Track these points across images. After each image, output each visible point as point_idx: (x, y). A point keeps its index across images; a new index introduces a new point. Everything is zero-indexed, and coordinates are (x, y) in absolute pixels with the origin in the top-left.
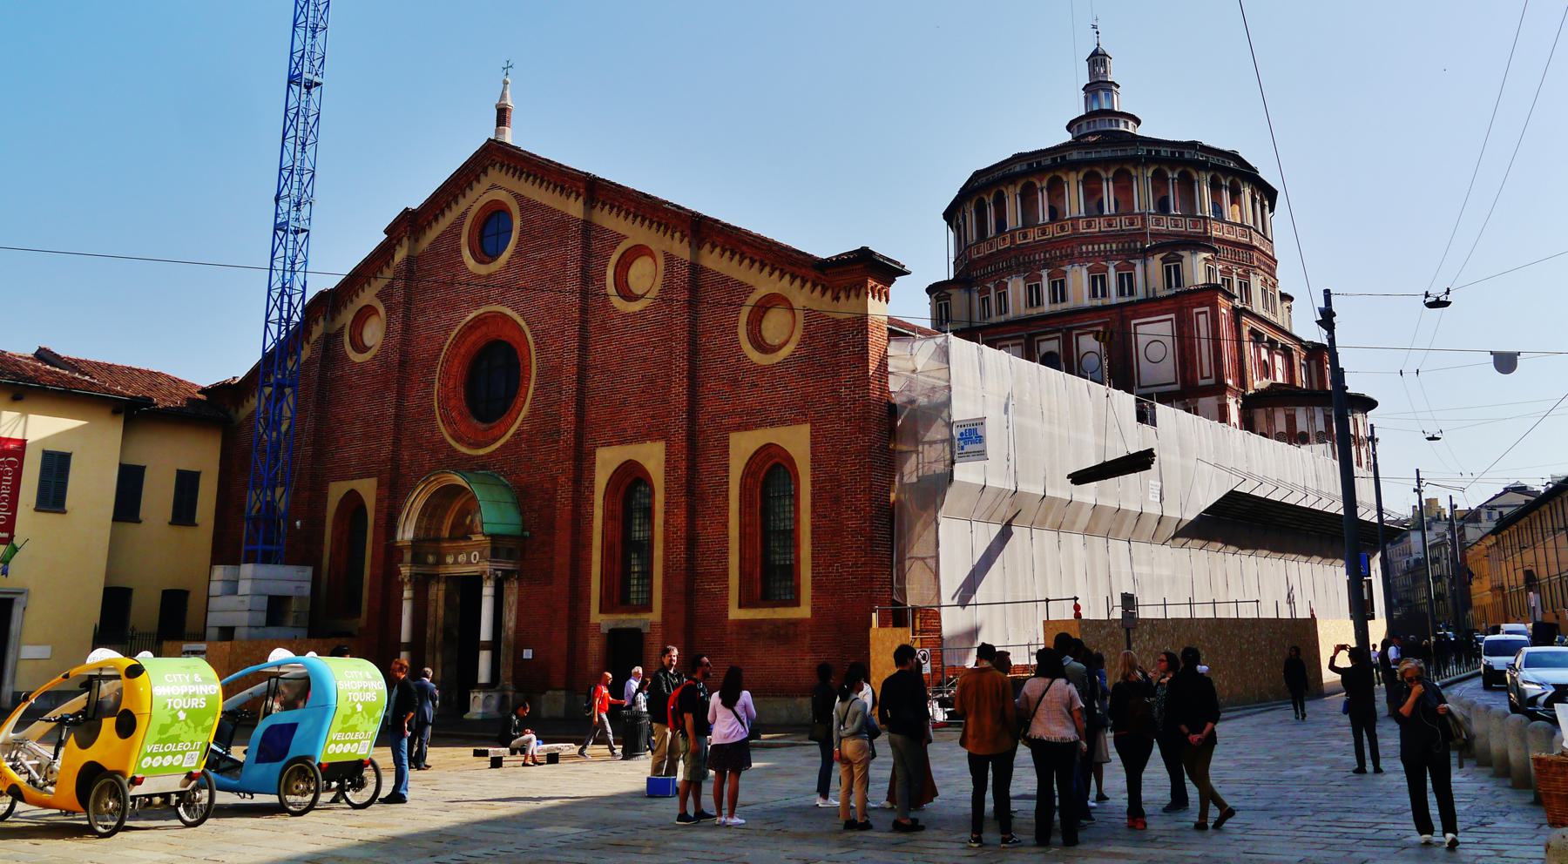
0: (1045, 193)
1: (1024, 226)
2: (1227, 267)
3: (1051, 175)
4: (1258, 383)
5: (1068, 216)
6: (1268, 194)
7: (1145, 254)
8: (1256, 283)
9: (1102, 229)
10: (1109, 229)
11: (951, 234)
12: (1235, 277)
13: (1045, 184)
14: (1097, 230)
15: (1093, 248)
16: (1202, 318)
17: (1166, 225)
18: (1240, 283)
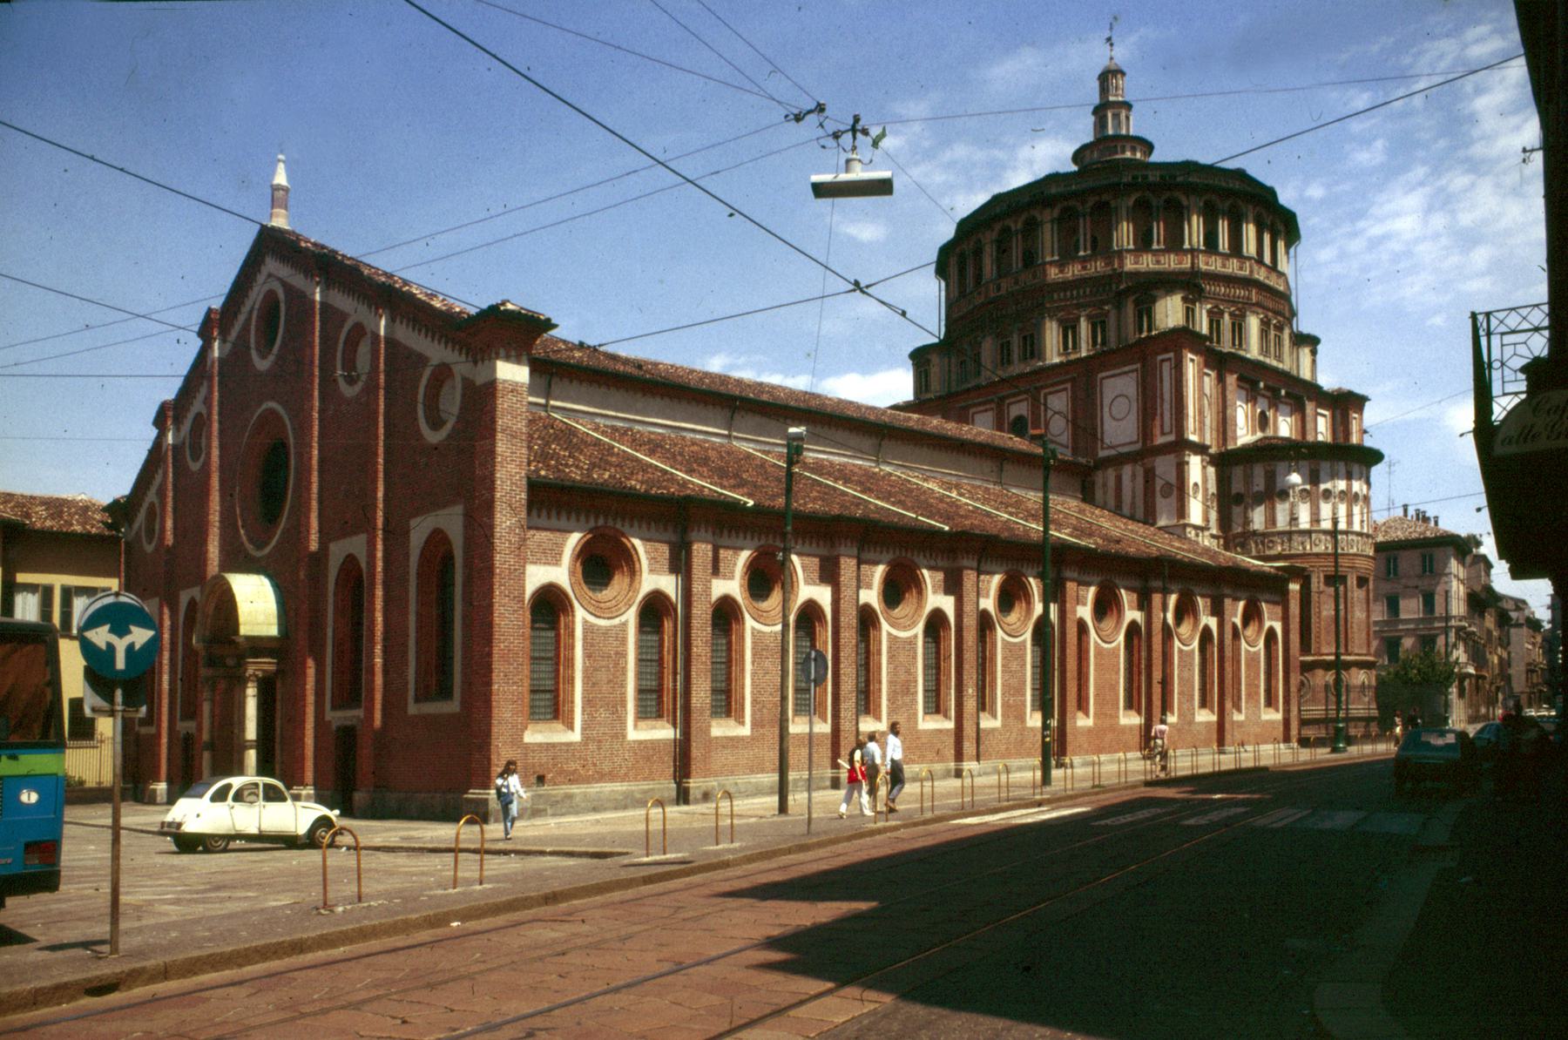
0: (1020, 237)
1: (1000, 276)
2: (1216, 307)
3: (1024, 217)
4: (1245, 435)
5: (1040, 261)
6: (1283, 225)
7: (1119, 299)
8: (1253, 323)
9: (1076, 272)
10: (1083, 273)
11: (943, 284)
12: (1226, 316)
13: (1020, 226)
14: (1070, 274)
15: (1065, 295)
16: (1166, 366)
17: (1147, 263)
18: (1233, 324)
